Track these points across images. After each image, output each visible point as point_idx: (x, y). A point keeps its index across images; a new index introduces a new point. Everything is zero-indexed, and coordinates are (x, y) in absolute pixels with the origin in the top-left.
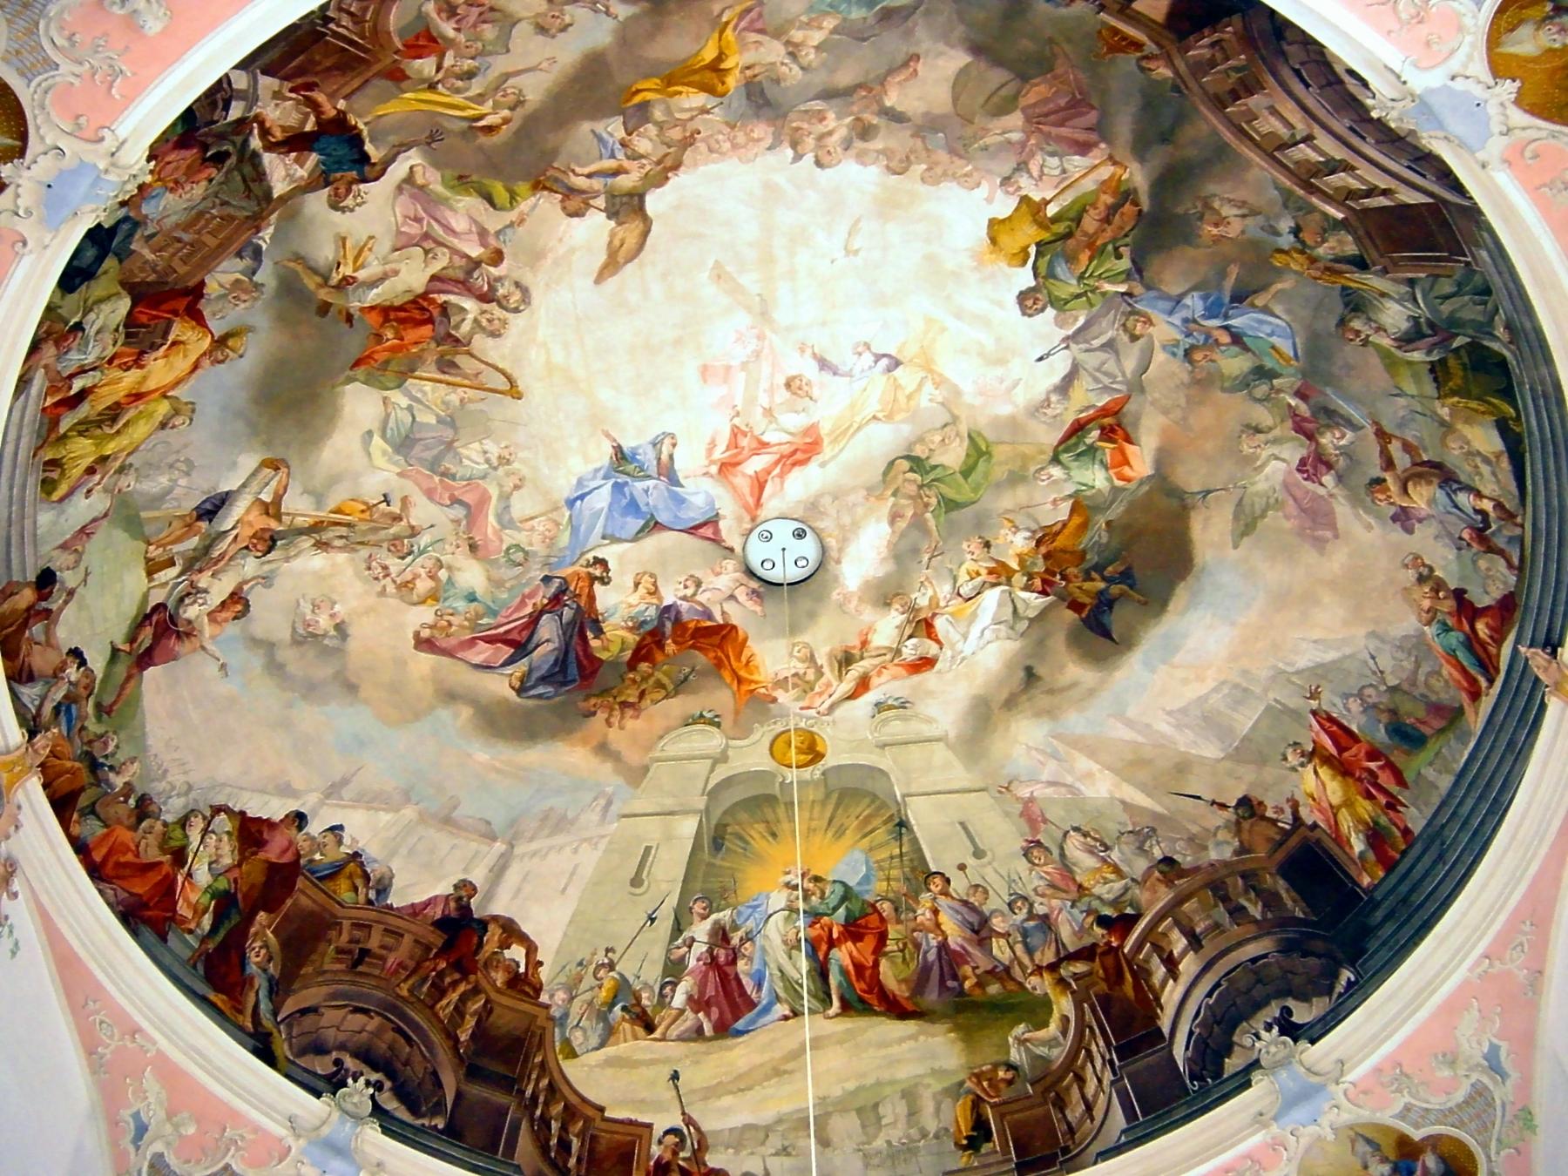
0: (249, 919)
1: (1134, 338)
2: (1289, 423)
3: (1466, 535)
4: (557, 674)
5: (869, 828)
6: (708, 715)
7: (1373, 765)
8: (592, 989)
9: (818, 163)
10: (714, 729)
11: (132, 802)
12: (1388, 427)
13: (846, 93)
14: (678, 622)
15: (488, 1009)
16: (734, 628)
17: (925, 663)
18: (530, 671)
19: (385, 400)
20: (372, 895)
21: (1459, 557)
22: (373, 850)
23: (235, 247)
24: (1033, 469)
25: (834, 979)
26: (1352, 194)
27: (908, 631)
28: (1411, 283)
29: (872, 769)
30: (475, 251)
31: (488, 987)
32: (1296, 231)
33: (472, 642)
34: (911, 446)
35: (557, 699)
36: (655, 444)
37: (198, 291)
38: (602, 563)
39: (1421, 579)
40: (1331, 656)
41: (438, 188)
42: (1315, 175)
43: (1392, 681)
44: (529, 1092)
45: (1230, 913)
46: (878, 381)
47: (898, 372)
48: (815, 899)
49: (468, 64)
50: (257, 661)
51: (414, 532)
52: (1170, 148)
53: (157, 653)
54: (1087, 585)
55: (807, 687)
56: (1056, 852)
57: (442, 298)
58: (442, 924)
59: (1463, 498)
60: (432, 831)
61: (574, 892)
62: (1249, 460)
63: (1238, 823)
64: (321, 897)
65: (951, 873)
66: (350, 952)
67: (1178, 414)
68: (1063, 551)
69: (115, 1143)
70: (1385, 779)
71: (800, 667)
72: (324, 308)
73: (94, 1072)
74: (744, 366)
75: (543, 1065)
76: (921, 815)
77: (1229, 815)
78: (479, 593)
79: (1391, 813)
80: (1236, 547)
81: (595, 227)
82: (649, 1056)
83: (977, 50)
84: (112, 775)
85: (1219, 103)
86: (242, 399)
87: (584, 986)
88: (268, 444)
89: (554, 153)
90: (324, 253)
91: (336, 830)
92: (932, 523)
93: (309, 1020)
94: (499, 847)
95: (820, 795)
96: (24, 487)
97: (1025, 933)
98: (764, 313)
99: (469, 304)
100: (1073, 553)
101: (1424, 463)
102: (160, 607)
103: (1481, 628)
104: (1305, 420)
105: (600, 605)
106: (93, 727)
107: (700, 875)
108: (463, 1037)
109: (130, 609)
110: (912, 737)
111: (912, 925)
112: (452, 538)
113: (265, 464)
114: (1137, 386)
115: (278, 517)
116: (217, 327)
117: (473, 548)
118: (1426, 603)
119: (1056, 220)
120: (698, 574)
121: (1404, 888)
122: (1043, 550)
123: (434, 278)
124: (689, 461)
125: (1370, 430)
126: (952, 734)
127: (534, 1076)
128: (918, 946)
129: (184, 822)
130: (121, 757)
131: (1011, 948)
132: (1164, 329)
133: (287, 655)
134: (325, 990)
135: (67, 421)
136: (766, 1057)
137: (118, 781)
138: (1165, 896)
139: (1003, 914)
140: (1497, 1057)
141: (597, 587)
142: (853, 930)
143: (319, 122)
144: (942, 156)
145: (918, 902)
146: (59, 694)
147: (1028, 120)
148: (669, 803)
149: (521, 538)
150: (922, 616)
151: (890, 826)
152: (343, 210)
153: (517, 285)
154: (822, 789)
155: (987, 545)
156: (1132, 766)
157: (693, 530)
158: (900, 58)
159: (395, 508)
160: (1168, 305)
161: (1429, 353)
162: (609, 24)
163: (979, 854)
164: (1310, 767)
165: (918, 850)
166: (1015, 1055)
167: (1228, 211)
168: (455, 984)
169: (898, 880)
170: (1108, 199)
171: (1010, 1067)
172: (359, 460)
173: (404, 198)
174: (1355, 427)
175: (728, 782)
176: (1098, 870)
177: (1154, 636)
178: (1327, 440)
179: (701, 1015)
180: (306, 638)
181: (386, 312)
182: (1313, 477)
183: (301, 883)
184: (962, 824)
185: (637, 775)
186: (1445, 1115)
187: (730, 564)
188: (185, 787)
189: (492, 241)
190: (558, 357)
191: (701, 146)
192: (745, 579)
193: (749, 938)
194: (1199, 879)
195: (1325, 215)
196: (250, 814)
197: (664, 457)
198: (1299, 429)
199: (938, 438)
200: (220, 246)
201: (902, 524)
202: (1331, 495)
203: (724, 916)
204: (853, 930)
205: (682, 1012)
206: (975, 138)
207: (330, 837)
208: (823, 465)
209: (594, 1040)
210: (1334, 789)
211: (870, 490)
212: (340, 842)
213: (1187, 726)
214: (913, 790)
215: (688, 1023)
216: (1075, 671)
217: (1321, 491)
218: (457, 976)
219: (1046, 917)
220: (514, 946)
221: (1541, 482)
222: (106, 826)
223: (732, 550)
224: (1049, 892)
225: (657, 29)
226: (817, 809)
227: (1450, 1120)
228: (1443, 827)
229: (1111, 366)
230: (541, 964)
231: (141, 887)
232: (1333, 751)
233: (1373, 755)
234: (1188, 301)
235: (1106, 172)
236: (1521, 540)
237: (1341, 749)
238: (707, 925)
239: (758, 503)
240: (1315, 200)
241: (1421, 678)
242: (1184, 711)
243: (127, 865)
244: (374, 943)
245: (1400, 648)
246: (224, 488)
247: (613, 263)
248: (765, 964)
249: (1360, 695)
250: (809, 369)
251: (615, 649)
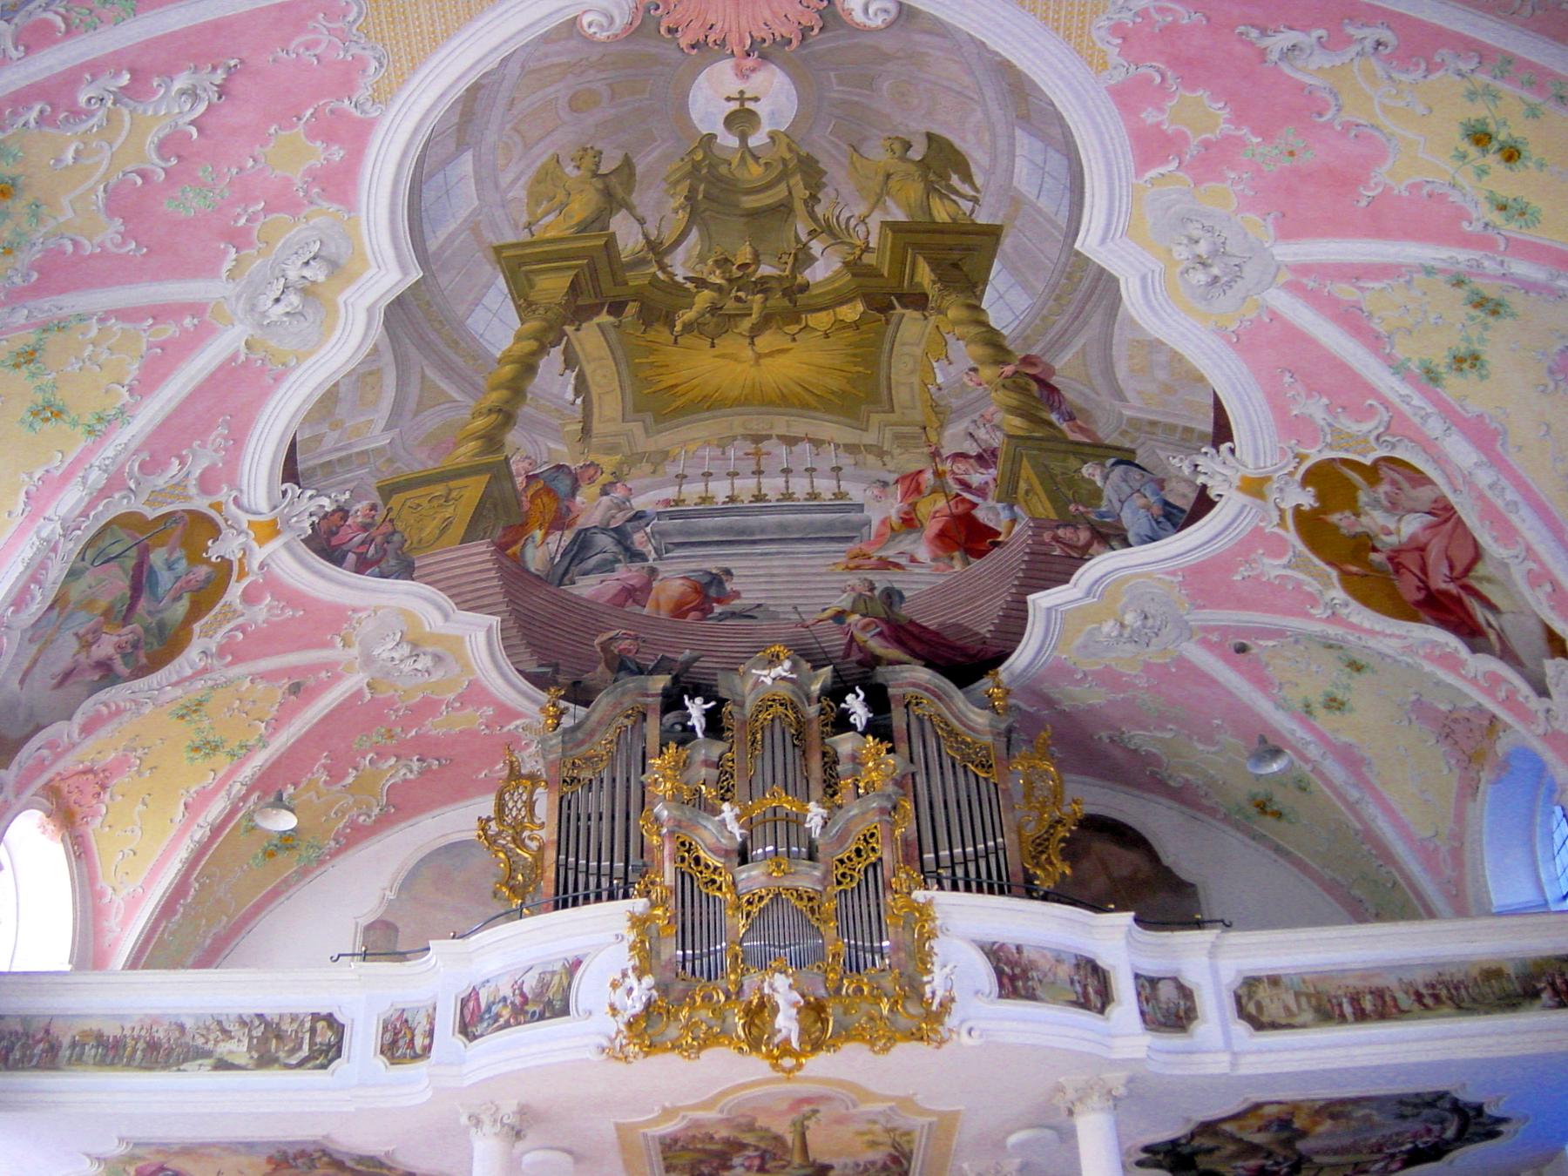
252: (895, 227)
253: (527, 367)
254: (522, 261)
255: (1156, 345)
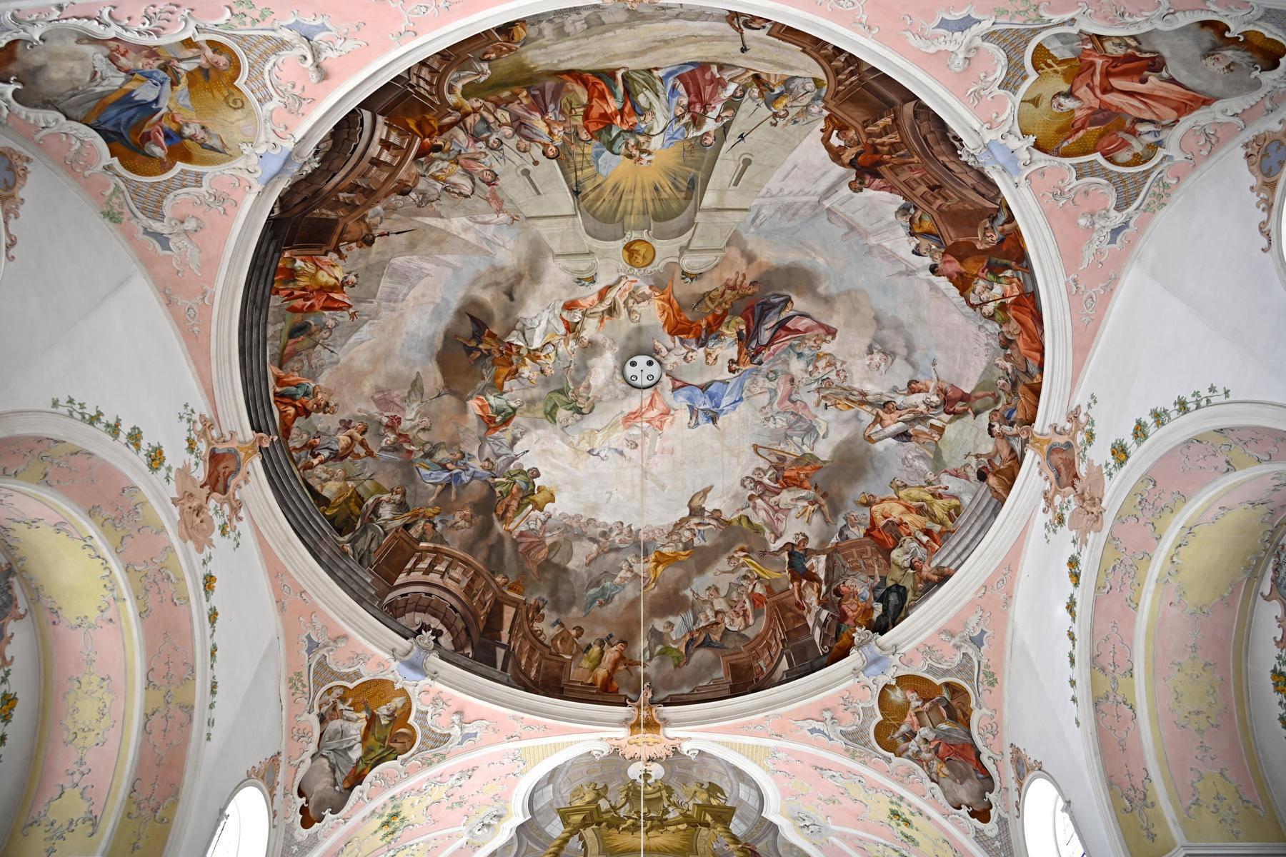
0: (984, 252)
1: (488, 460)
2: (411, 437)
3: (318, 440)
4: (767, 308)
5: (598, 190)
6: (688, 279)
7: (309, 303)
8: (792, 107)
9: (622, 523)
10: (686, 270)
11: (1009, 352)
12: (370, 459)
13: (611, 550)
14: (698, 339)
15: (865, 124)
16: (669, 333)
17: (570, 306)
18: (780, 312)
19: (812, 450)
20: (912, 211)
21: (316, 428)
22: (902, 232)
23: (847, 542)
24: (525, 406)
25: (620, 88)
26: (420, 559)
27: (579, 326)
28: (386, 534)
29: (595, 237)
30: (759, 501)
31: (862, 133)
32: (434, 526)
33: (806, 330)
34: (582, 419)
35: (769, 294)
36: (697, 424)
37: (868, 533)
38: (731, 371)
39: (327, 404)
40: (352, 340)
41: (767, 531)
42: (435, 558)
43: (319, 348)
44: (854, 78)
45: (358, 186)
46: (596, 445)
47: (589, 448)
48: (632, 142)
49: (744, 583)
50: (917, 356)
51: (818, 390)
52: (490, 543)
53: (959, 395)
54: (488, 347)
55: (635, 296)
56: (477, 180)
57: (777, 485)
58: (878, 175)
59: (326, 454)
60: (864, 226)
61: (788, 165)
62: (424, 415)
63: (370, 230)
64: (942, 228)
65: (542, 159)
66: (940, 194)
67: (462, 429)
68: (504, 366)
69: (1139, 232)
70: (299, 303)
71: (636, 307)
72: (824, 496)
73: (1116, 279)
74: (655, 454)
75: (840, 83)
76: (566, 202)
77: (376, 232)
78: (795, 358)
79: (288, 292)
80: (418, 373)
81: (709, 506)
82: (761, 63)
83: (565, 570)
84: (1010, 371)
85: (477, 573)
86: (871, 475)
87: (798, 110)
88: (868, 450)
89: (721, 535)
90: (817, 519)
91: (916, 252)
92: (570, 384)
93: (983, 190)
94: (827, 204)
95: (627, 219)
96: (965, 524)
97: (489, 128)
98: (645, 473)
99: (766, 481)
100: (499, 365)
101: (348, 455)
102: (948, 413)
103: (291, 410)
104: (405, 442)
105: (736, 348)
106: (1004, 399)
107: (706, 162)
108: (888, 120)
109: (958, 424)
110: (573, 259)
111: (567, 125)
112: (801, 385)
113: (874, 442)
114: (482, 440)
115: (878, 415)
116: (867, 511)
117: (792, 380)
118: (319, 396)
119: (528, 504)
120: (684, 363)
121: (265, 271)
122: (514, 367)
123: (778, 494)
124: (686, 415)
125: (376, 452)
126: (550, 259)
127: (848, 82)
128: (562, 112)
129: (991, 317)
130: (1001, 373)
131: (497, 118)
132: (476, 465)
133: (902, 351)
134: (964, 192)
135: (937, 528)
136: (673, 50)
137: (1008, 365)
138: (402, 174)
139: (506, 137)
140: (160, 242)
141: (736, 359)
142: (606, 121)
143: (801, 582)
144: (575, 525)
145: (563, 139)
146: (1006, 428)
147: (544, 542)
148: (718, 218)
149: (768, 384)
150: (571, 335)
151: (583, 194)
152: (804, 535)
153: (745, 487)
154: (626, 224)
155: (542, 371)
156: (442, 240)
157: (685, 385)
158: (592, 564)
159: (823, 402)
160: (476, 475)
161: (367, 507)
162: (693, 587)
163: (526, 173)
164: (341, 279)
165: (564, 174)
166: (485, 66)
167: (462, 523)
168: (883, 144)
169: (578, 154)
170: (509, 515)
171: (488, 60)
172: (832, 426)
173: (781, 530)
174: (383, 449)
175: (681, 232)
176: (448, 176)
177: (447, 319)
178: (392, 437)
179: (718, 76)
180: (889, 354)
181: (800, 486)
182: (392, 418)
183: (950, 243)
184: (539, 194)
185: (734, 239)
186: (168, 188)
187: (669, 368)
188: (982, 330)
189: (751, 504)
190: (734, 460)
191: (666, 532)
192: (662, 359)
193: (678, 118)
194: (383, 192)
195: (426, 541)
196: (958, 292)
197: (694, 418)
198: (406, 436)
199: (570, 421)
200: (853, 547)
201: (584, 384)
202: (382, 414)
203: (693, 133)
204: (606, 121)
205: (732, 80)
206: (563, 532)
207: (922, 250)
208: (622, 412)
209: (798, 81)
210: (324, 277)
211: (600, 401)
212: (918, 246)
213: (416, 270)
214: (571, 220)
215: (729, 73)
216: (486, 296)
217: (386, 414)
218: (879, 147)
219: (476, 141)
220: (836, 145)
221: (303, 498)
222: (1026, 360)
223: (667, 375)
224: (477, 156)
225: (678, 581)
226: (629, 208)
227: (162, 187)
228: (260, 313)
229: (496, 448)
230: (822, 130)
231: (1030, 323)
232: (332, 295)
233: (312, 306)
234: (468, 478)
235: (512, 526)
236: (296, 464)
237: (329, 298)
238: (705, 129)
239: (653, 396)
240: (432, 545)
241: (306, 362)
242: (420, 278)
243: (1029, 337)
244: (923, 189)
245: (321, 366)
246: (894, 442)
247: (705, 492)
248: (668, 101)
249: (330, 330)
250: (627, 451)
251: (733, 323)
252: (698, 805)
253: (566, 841)
254: (566, 812)
255: (792, 845)
